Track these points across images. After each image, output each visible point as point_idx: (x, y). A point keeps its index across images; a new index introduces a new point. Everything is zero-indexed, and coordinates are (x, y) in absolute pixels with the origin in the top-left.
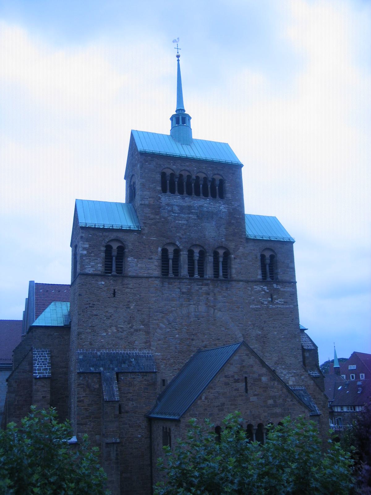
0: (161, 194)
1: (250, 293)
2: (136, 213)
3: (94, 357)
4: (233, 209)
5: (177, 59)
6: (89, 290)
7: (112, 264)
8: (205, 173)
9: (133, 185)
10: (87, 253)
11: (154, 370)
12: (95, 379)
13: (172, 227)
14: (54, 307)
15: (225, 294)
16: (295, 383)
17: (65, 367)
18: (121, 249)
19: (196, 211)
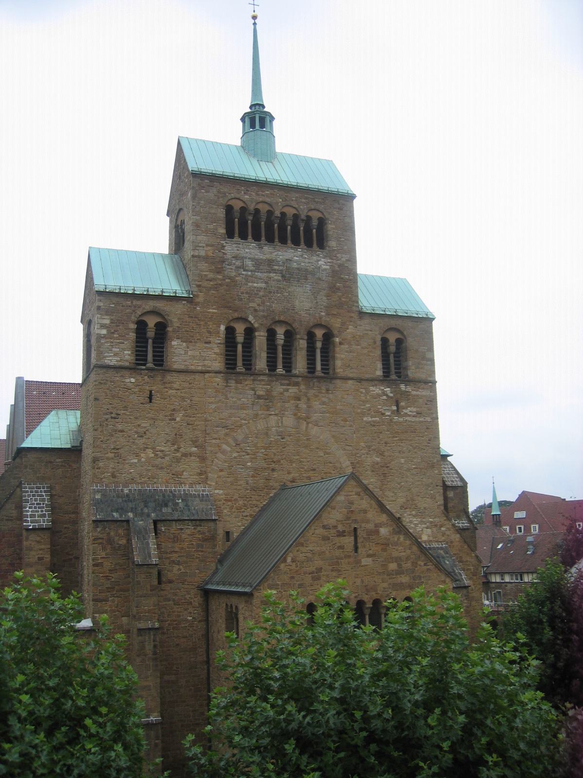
1: (363, 398)
2: (185, 269)
3: (118, 497)
4: (339, 266)
5: (253, 21)
6: (111, 391)
7: (146, 351)
8: (295, 208)
9: (181, 225)
10: (108, 333)
11: (212, 517)
12: (121, 531)
13: (242, 293)
14: (55, 418)
15: (324, 399)
16: (431, 539)
17: (73, 513)
18: (161, 327)
19: (281, 268)
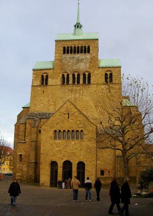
18: (47, 76)
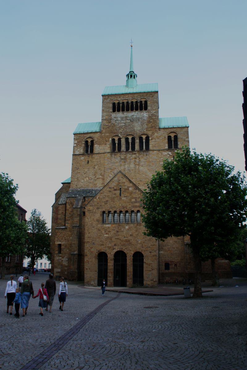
0: (112, 113)
18: (92, 142)
